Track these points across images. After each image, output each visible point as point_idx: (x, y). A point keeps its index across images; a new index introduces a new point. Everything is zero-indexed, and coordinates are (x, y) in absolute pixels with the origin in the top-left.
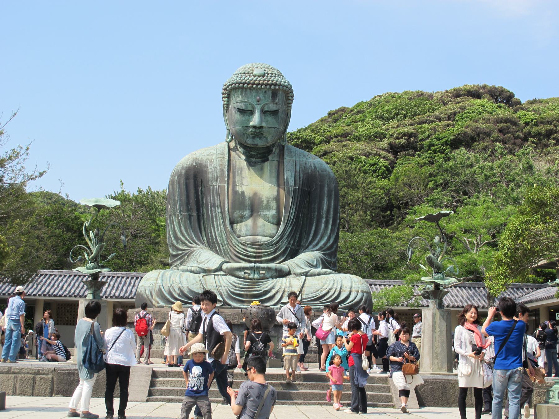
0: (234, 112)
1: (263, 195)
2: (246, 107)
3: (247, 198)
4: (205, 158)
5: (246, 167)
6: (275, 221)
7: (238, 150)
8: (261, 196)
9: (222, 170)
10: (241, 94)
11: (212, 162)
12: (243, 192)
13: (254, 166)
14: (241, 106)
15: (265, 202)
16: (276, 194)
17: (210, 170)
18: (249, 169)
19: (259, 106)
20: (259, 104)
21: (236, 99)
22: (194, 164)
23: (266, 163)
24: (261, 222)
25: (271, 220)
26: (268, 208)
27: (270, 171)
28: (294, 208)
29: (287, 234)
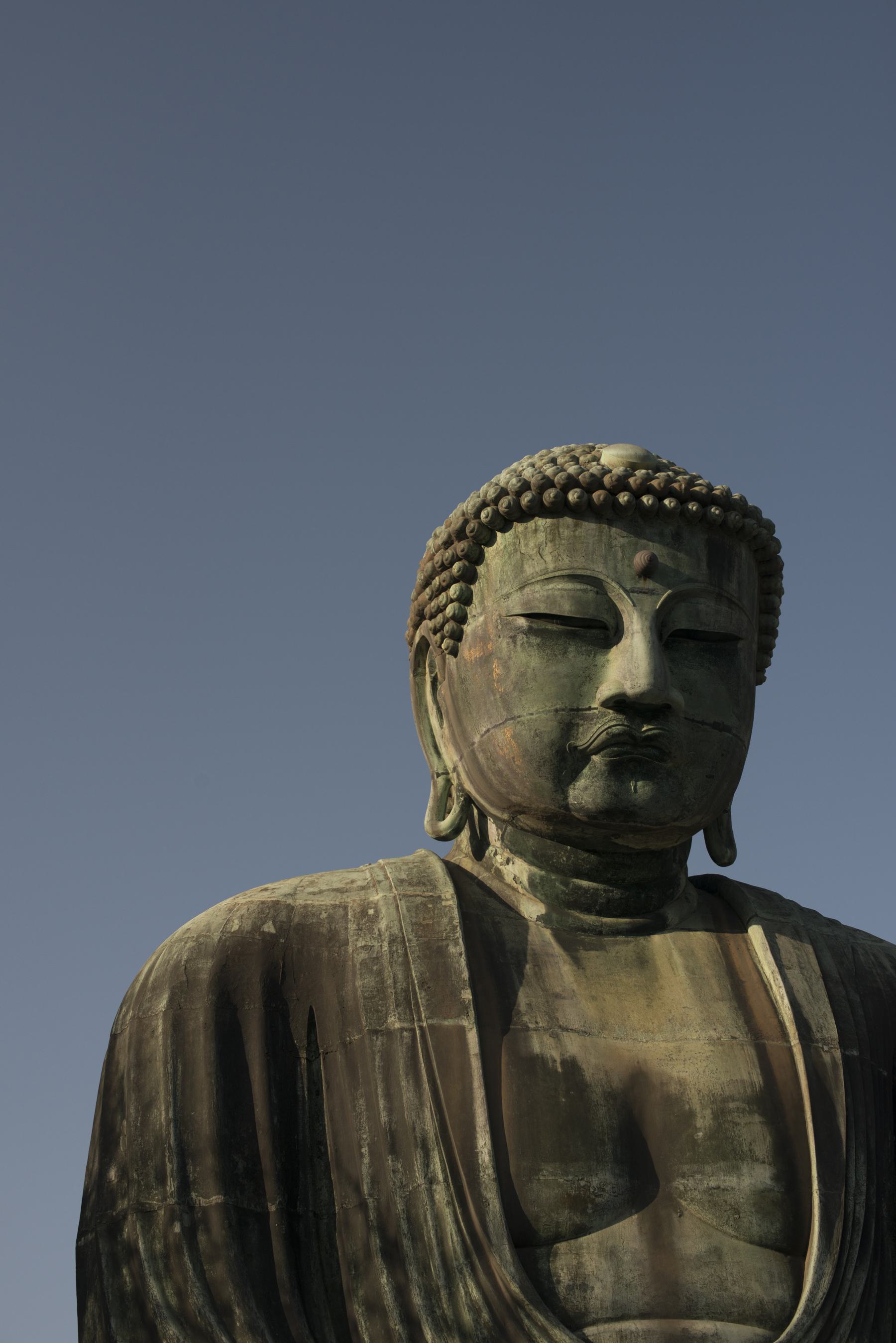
0: (504, 644)
1: (681, 1083)
2: (577, 601)
3: (597, 1094)
4: (328, 900)
5: (557, 949)
6: (773, 1228)
7: (499, 874)
8: (673, 1089)
9: (434, 952)
10: (554, 535)
11: (366, 917)
12: (571, 1066)
13: (601, 947)
14: (550, 600)
15: (703, 1121)
16: (757, 1078)
17: (363, 955)
18: (577, 962)
19: (647, 600)
20: (651, 592)
21: (519, 569)
22: (269, 928)
23: (657, 939)
24: (693, 1234)
25: (754, 1223)
26: (725, 1151)
27: (692, 971)
28: (862, 1158)
29: (853, 1307)
